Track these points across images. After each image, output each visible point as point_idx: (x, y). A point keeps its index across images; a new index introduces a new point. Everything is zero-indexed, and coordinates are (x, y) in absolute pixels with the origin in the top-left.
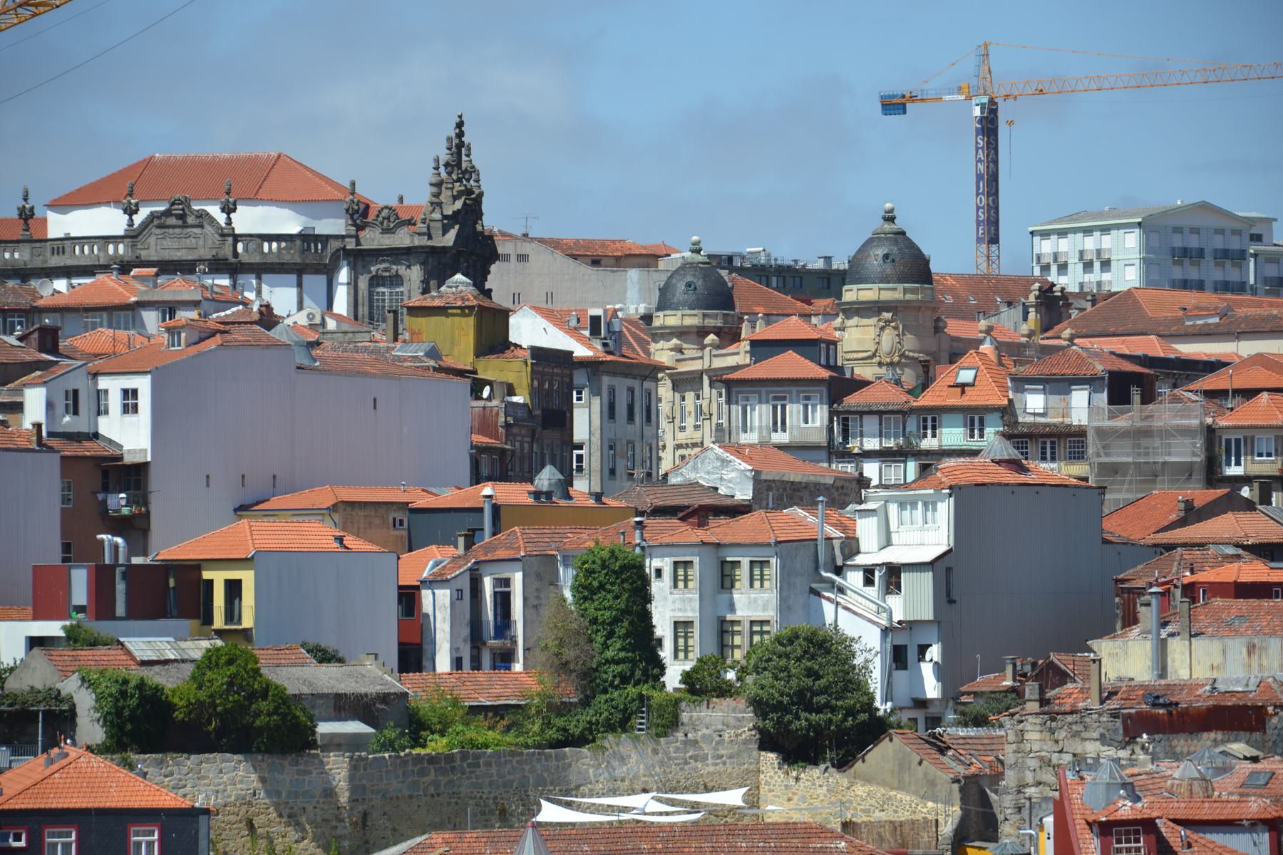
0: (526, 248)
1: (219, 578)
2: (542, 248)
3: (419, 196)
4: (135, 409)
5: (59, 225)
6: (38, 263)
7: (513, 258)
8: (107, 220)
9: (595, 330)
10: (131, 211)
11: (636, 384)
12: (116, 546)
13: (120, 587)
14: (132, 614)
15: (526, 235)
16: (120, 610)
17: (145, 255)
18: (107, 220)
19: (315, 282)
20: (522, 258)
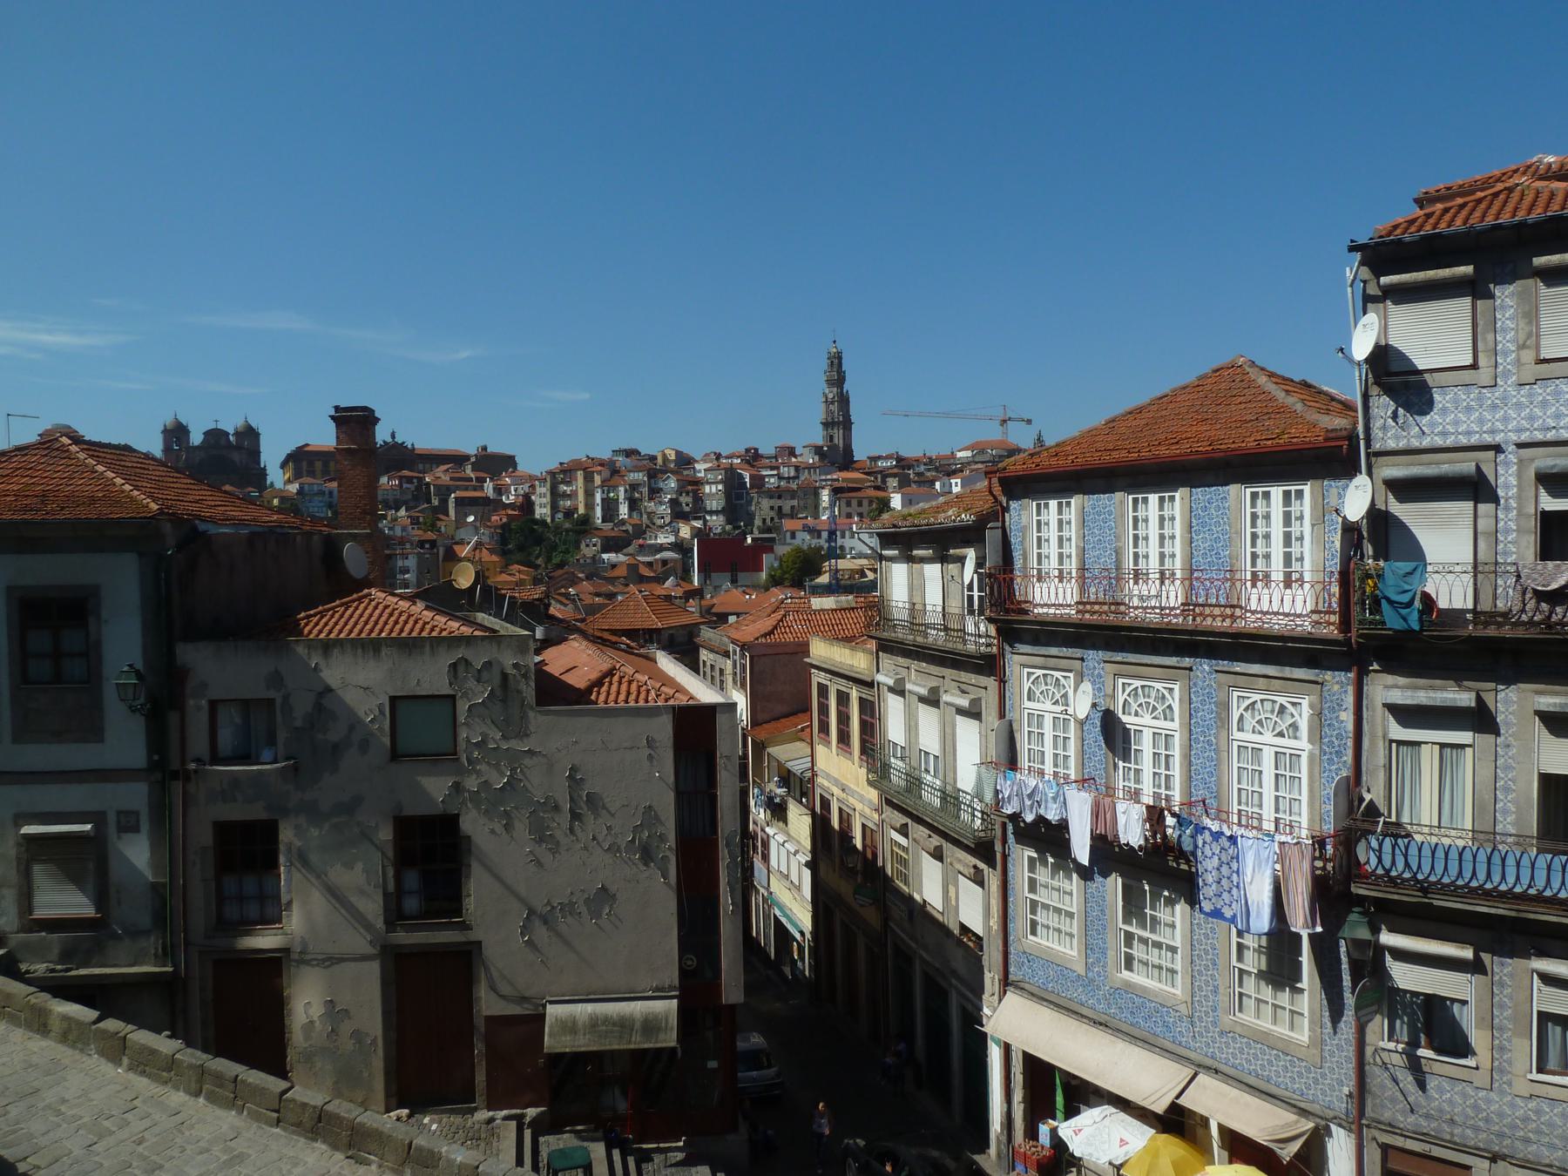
5: (959, 455)
8: (968, 454)
18: (968, 454)
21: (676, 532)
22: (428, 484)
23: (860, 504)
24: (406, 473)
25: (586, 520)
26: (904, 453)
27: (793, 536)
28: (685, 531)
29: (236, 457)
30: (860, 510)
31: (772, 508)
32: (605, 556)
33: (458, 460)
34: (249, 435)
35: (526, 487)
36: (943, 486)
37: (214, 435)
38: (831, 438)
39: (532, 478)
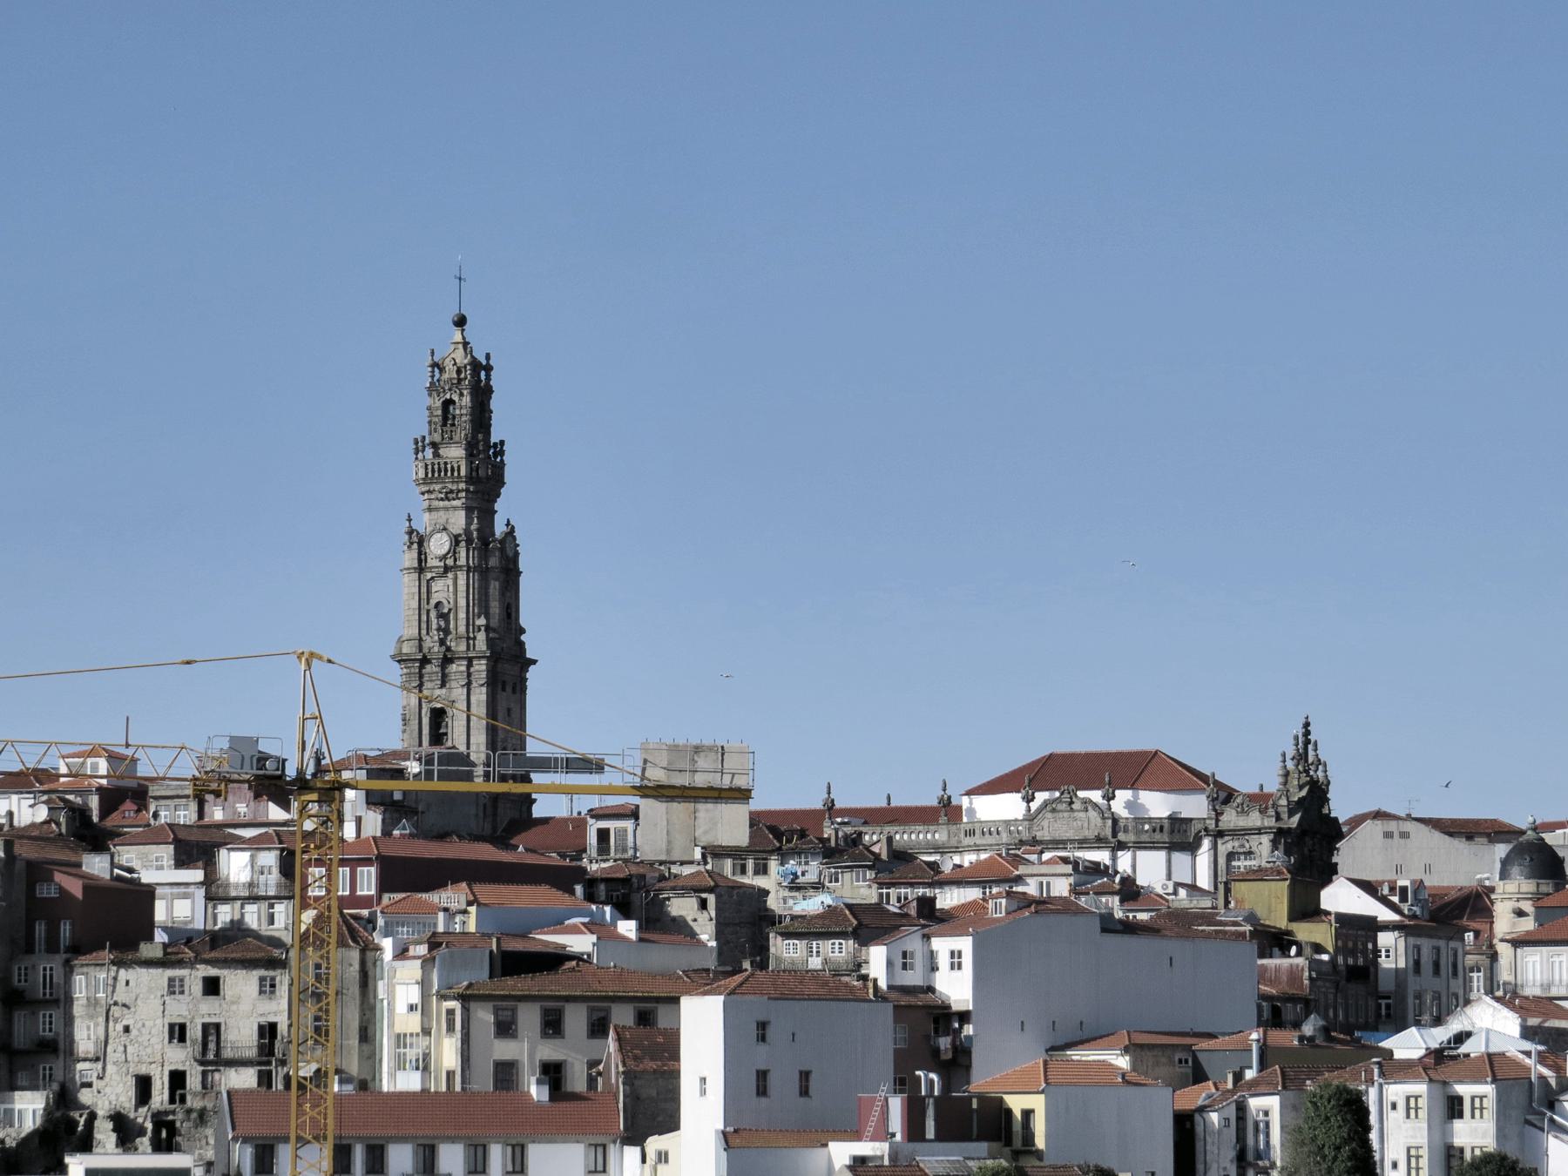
0: (1410, 827)
1: (1016, 1103)
2: (1422, 826)
3: (1273, 785)
4: (960, 967)
6: (954, 842)
7: (1396, 835)
9: (1404, 899)
10: (1029, 799)
11: (1442, 943)
12: (932, 1081)
13: (930, 1112)
14: (941, 1136)
15: (1409, 816)
16: (930, 1133)
17: (1039, 835)
19: (1181, 859)
20: (1404, 835)
23: (553, 1025)
30: (550, 1051)
31: (178, 1032)
38: (438, 716)
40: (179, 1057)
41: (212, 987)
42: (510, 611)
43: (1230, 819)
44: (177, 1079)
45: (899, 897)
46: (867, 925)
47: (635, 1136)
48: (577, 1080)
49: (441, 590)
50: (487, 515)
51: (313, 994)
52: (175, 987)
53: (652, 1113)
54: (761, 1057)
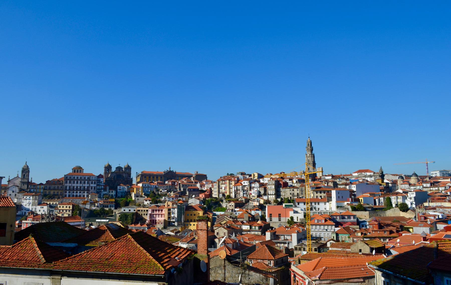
18: (356, 174)
21: (258, 201)
22: (180, 184)
24: (173, 180)
25: (229, 197)
26: (334, 174)
27: (298, 204)
28: (262, 202)
29: (124, 175)
30: (321, 195)
31: (291, 194)
32: (236, 209)
33: (189, 176)
34: (128, 168)
35: (210, 186)
36: (350, 187)
37: (119, 168)
39: (212, 182)
40: (291, 196)
41: (293, 190)
42: (314, 160)
43: (375, 175)
44: (291, 197)
45: (348, 182)
46: (346, 184)
47: (328, 202)
48: (323, 197)
49: (309, 158)
50: (312, 152)
51: (302, 191)
52: (290, 190)
53: (329, 199)
54: (339, 195)
